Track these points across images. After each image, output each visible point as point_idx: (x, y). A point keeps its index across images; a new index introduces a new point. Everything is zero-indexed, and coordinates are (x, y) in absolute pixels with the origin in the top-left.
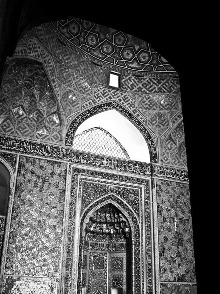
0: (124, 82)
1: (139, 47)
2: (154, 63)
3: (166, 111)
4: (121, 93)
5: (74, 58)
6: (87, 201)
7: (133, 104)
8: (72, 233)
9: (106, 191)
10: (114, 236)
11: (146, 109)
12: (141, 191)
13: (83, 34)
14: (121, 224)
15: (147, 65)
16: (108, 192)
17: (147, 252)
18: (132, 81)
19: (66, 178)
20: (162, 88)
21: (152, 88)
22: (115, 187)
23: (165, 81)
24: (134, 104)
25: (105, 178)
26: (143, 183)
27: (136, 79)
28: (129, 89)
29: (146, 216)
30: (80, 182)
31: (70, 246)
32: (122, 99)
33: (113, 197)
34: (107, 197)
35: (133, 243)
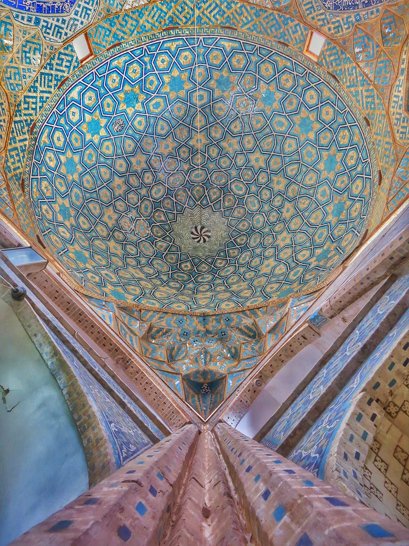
0: (72, 56)
1: (87, 120)
2: (62, 120)
3: (6, 64)
4: (69, 35)
5: (146, 24)
7: (45, 33)
11: (27, 41)
13: (149, 67)
15: (66, 108)
18: (64, 69)
20: (34, 95)
21: (43, 82)
23: (38, 108)
24: (45, 35)
27: (61, 77)
28: (62, 51)
32: (63, 26)
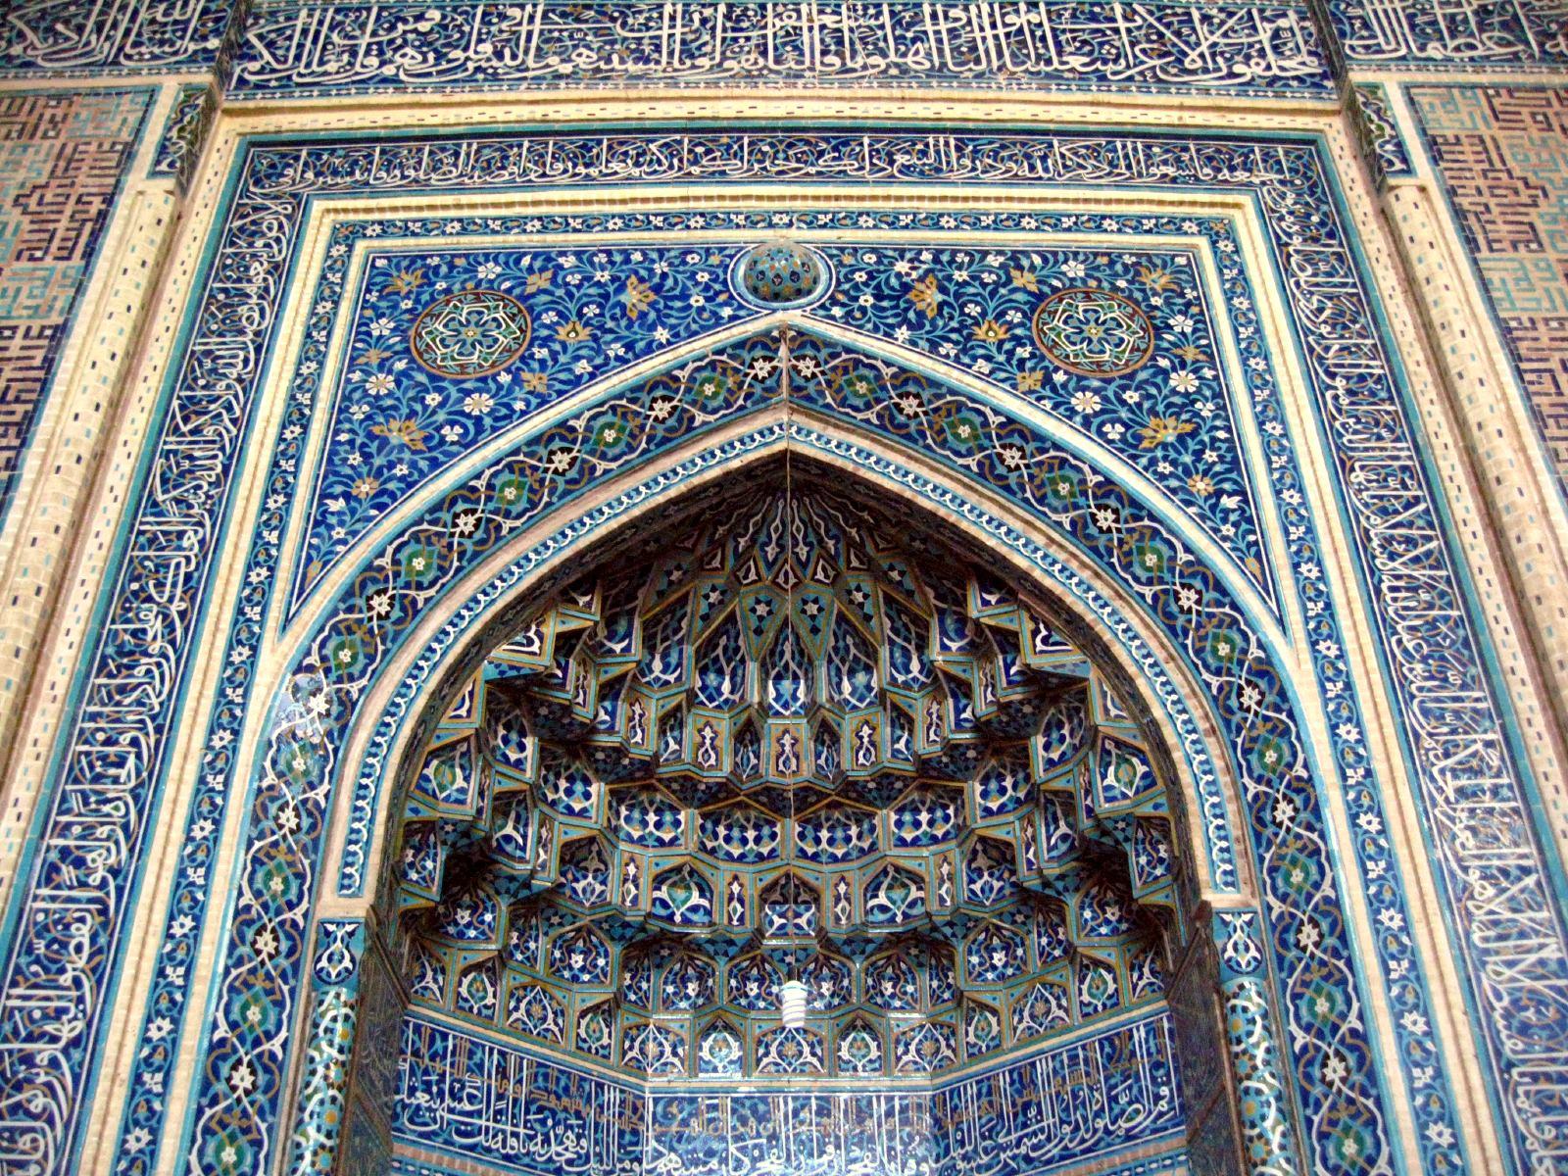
6: (395, 439)
8: (99, 861)
9: (697, 300)
10: (999, 958)
12: (1231, 264)
14: (1039, 740)
16: (726, 312)
17: (1511, 1045)
19: (103, 217)
22: (824, 248)
25: (673, 174)
26: (1241, 176)
29: (1378, 527)
30: (335, 266)
31: (44, 1052)
33: (807, 367)
34: (712, 366)
35: (1238, 947)
